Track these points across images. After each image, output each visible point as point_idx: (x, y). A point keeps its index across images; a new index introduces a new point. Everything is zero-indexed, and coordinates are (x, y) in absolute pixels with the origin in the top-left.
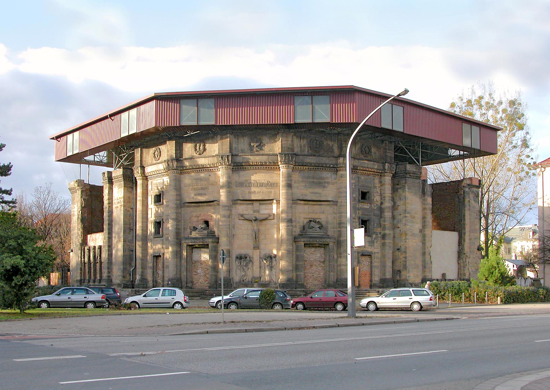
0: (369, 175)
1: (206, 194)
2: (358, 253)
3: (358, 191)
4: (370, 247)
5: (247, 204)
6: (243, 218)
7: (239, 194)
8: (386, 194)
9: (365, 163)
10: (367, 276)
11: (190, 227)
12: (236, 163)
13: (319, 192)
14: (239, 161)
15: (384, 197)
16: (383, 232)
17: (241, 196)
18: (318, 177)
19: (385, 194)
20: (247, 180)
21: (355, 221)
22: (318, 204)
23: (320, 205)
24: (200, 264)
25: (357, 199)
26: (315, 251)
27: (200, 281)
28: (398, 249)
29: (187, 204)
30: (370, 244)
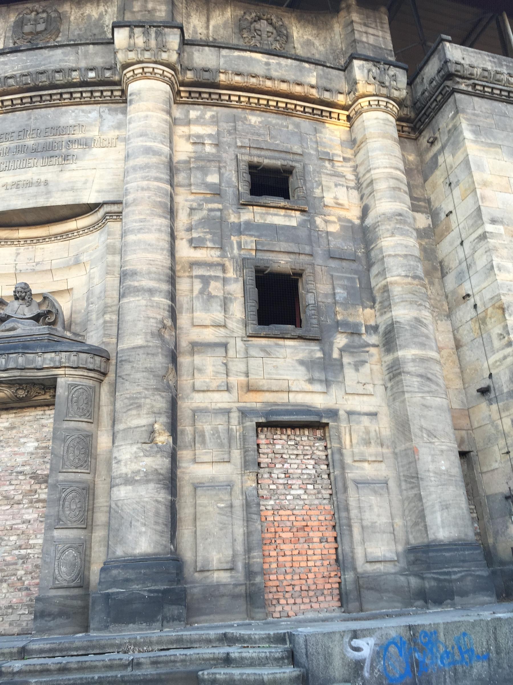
0: (286, 113)
2: (244, 413)
3: (234, 163)
4: (318, 387)
8: (372, 172)
9: (258, 61)
10: (316, 536)
13: (43, 178)
15: (371, 183)
16: (383, 321)
18: (43, 127)
19: (369, 171)
21: (220, 274)
22: (56, 236)
23: (61, 235)
25: (230, 192)
26: (12, 428)
28: (484, 391)
30: (317, 375)
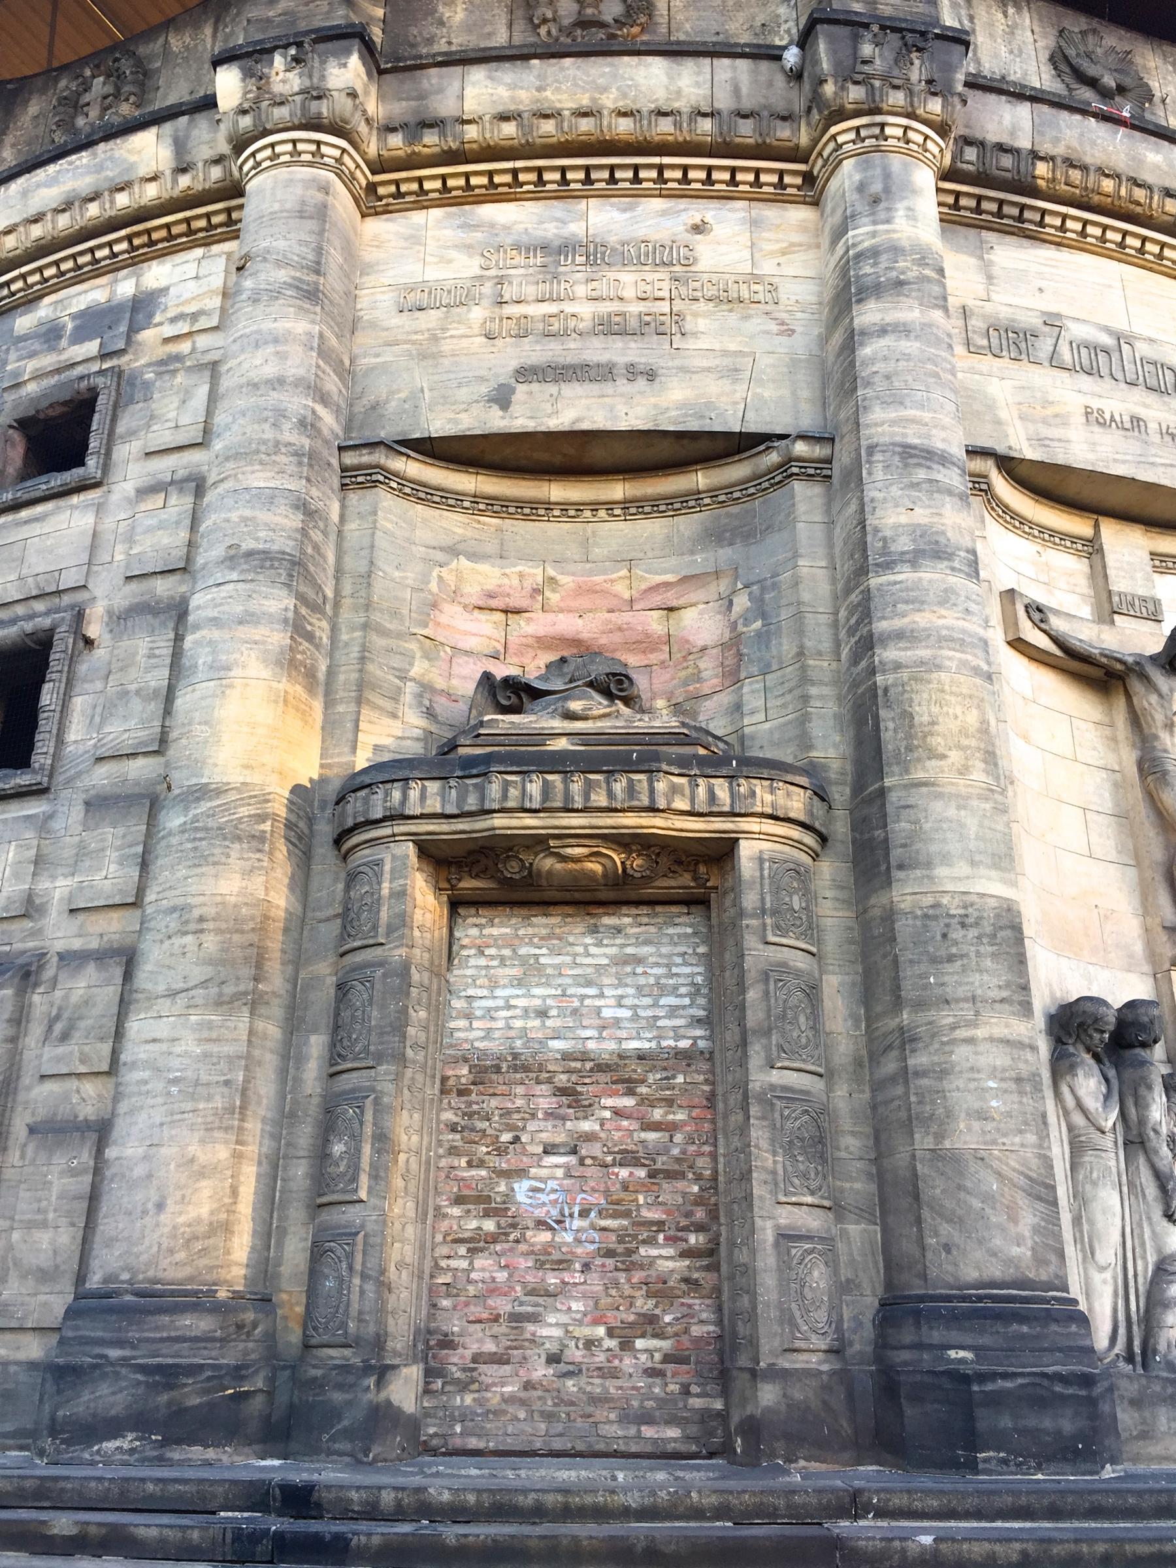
1: (651, 375)
5: (1043, 529)
6: (1042, 642)
7: (1003, 414)
11: (426, 688)
12: (981, 144)
14: (1005, 139)
17: (1023, 437)
20: (1058, 316)
24: (545, 1103)
27: (550, 1330)
29: (414, 468)
